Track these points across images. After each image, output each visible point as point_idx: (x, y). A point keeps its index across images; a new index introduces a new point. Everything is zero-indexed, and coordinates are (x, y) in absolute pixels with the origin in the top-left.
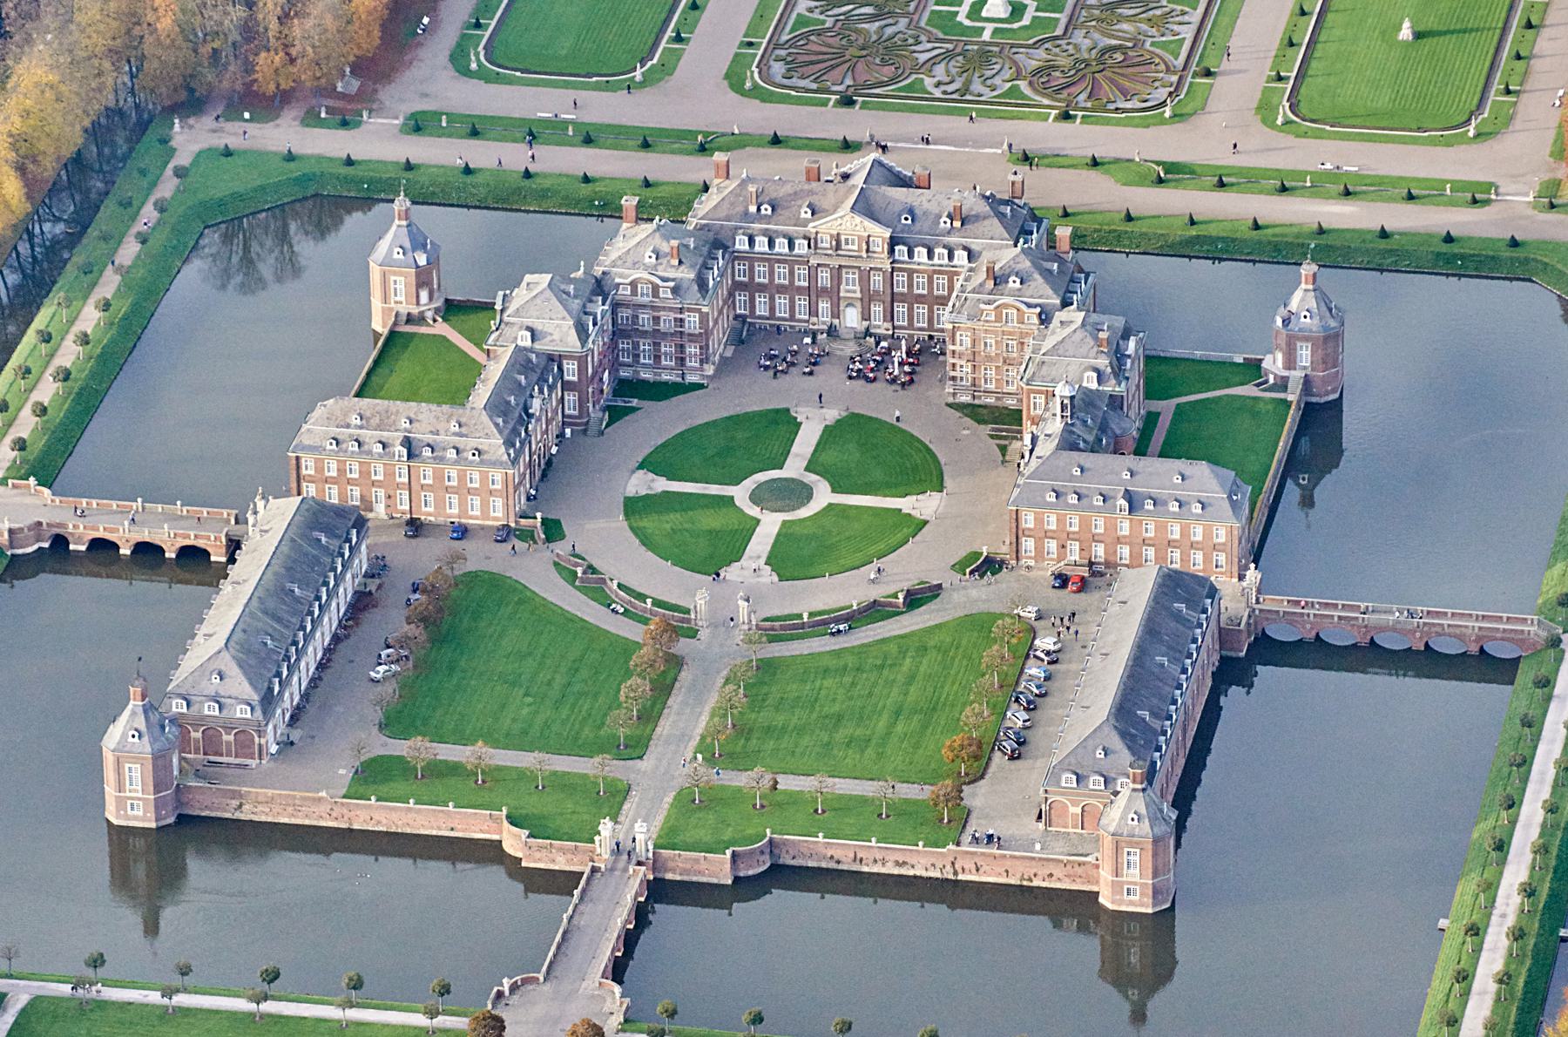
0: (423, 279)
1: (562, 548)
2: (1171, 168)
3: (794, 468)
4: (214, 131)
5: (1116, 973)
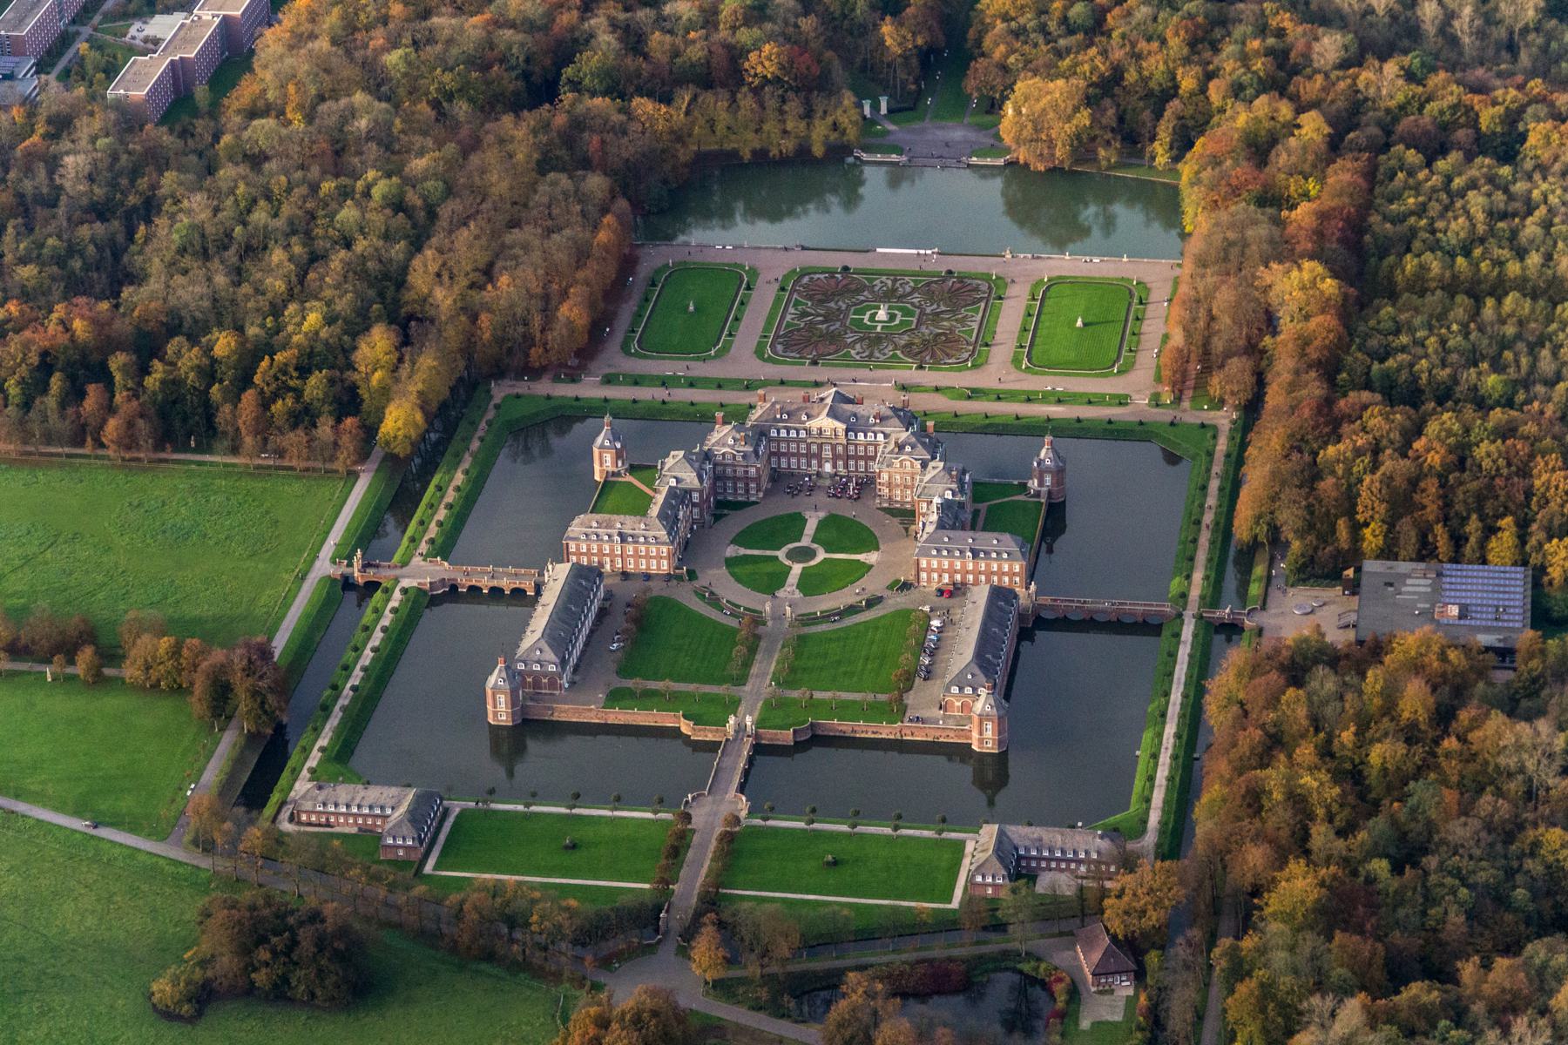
0: (619, 455)
1: (696, 584)
2: (974, 391)
3: (805, 542)
5: (981, 782)
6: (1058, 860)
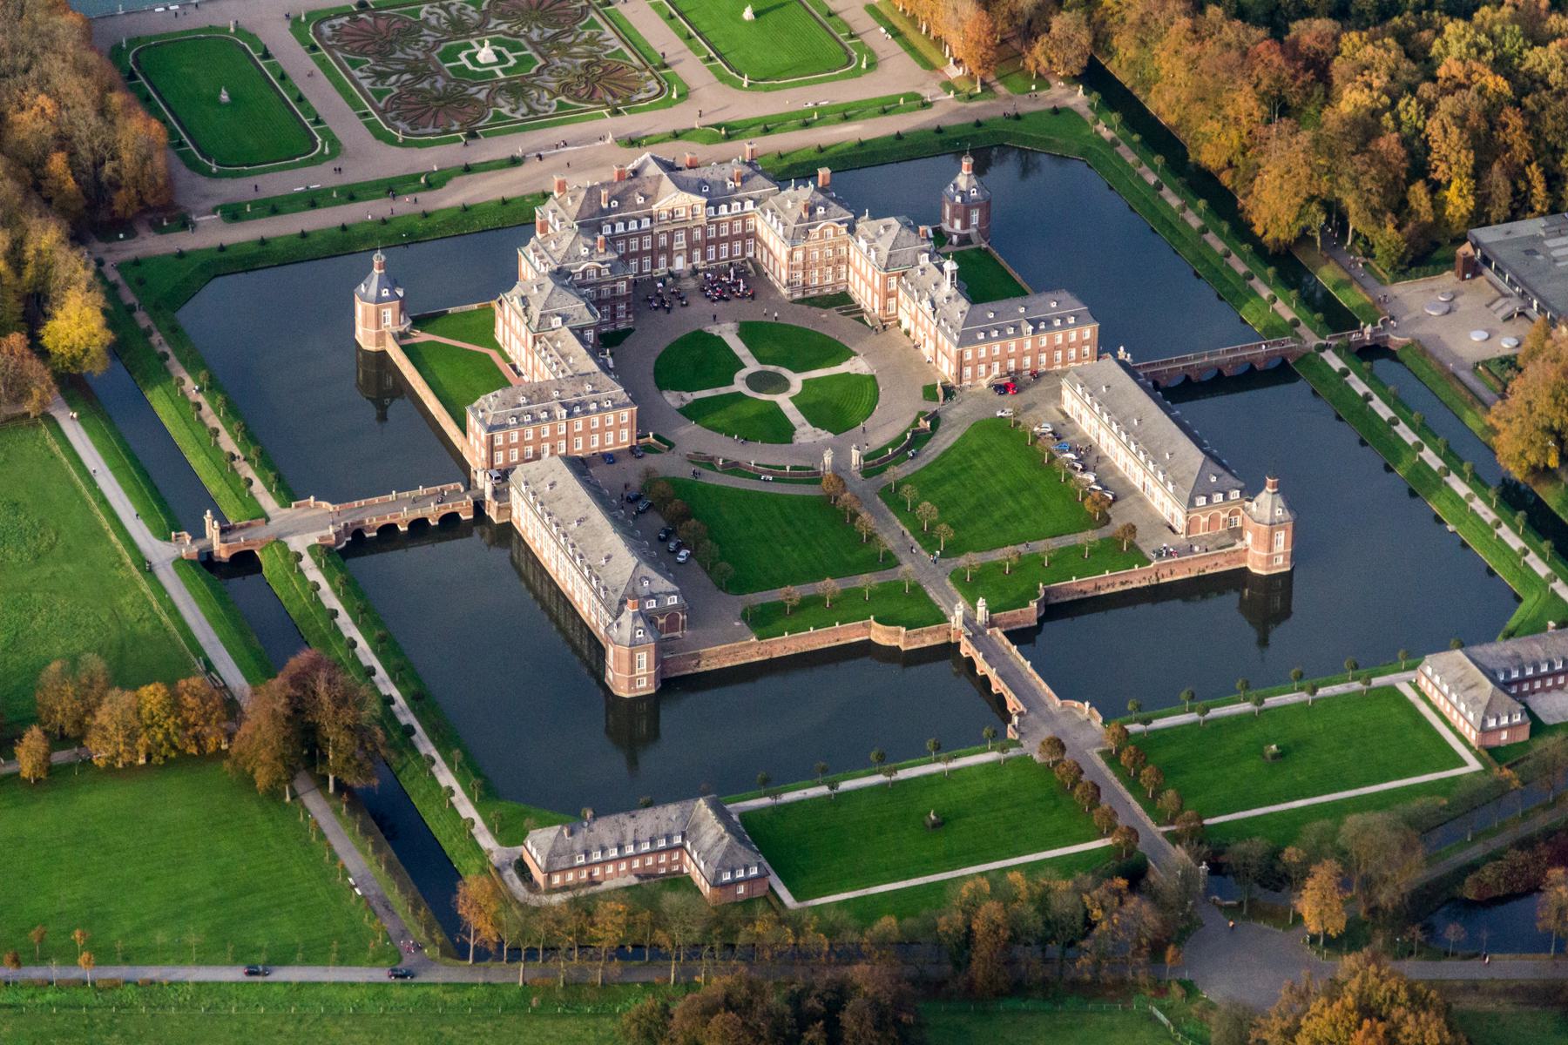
0: (402, 309)
2: (728, 127)
4: (109, 251)
6: (1544, 677)
